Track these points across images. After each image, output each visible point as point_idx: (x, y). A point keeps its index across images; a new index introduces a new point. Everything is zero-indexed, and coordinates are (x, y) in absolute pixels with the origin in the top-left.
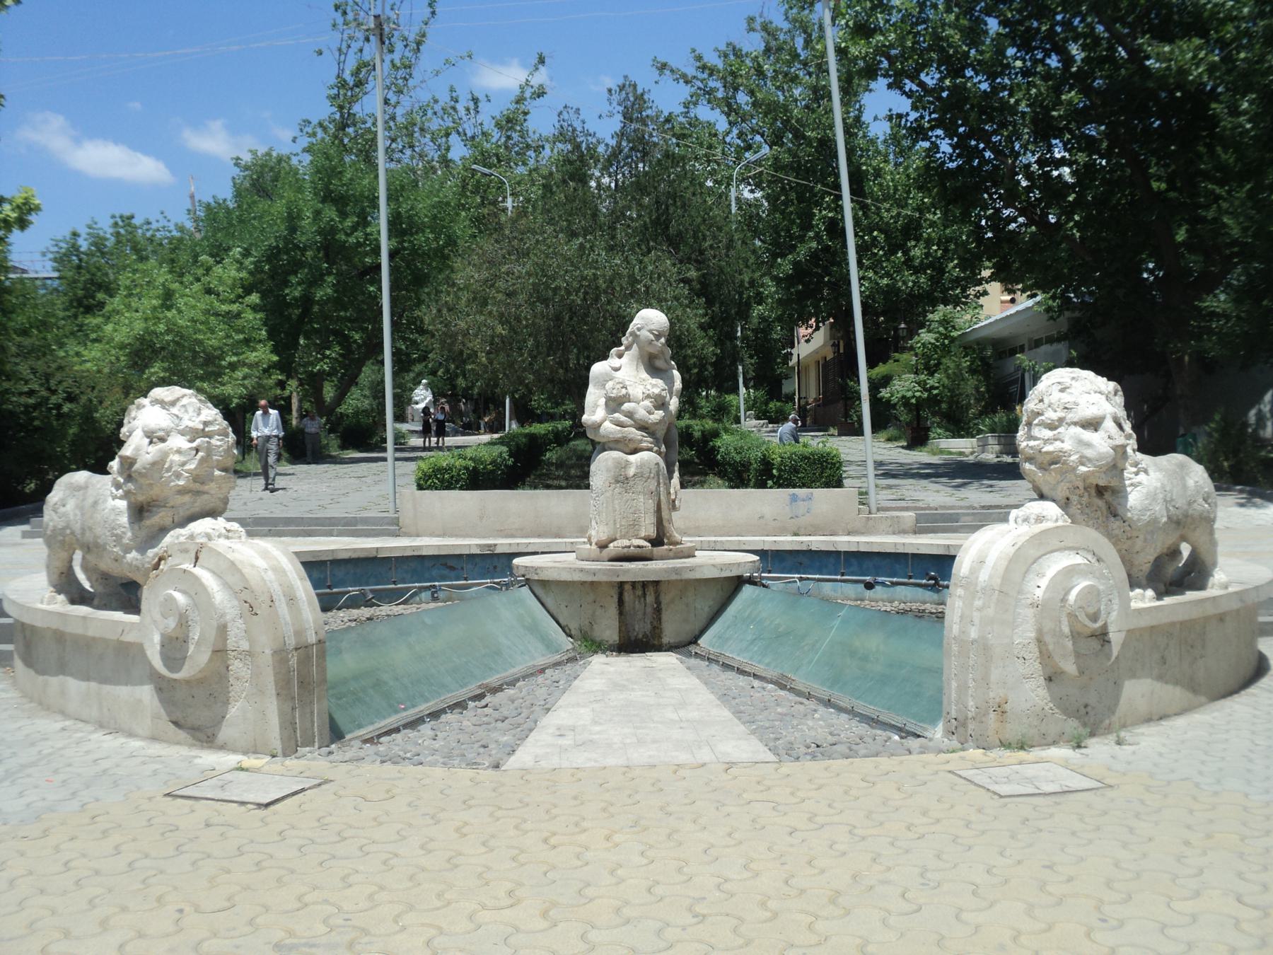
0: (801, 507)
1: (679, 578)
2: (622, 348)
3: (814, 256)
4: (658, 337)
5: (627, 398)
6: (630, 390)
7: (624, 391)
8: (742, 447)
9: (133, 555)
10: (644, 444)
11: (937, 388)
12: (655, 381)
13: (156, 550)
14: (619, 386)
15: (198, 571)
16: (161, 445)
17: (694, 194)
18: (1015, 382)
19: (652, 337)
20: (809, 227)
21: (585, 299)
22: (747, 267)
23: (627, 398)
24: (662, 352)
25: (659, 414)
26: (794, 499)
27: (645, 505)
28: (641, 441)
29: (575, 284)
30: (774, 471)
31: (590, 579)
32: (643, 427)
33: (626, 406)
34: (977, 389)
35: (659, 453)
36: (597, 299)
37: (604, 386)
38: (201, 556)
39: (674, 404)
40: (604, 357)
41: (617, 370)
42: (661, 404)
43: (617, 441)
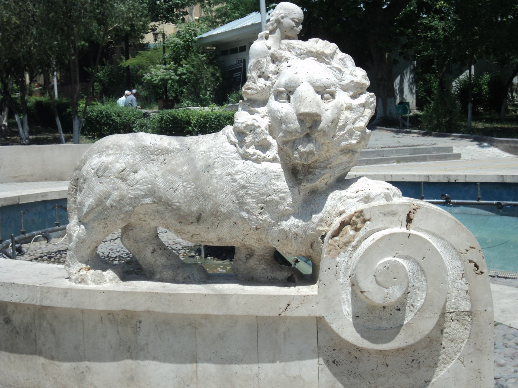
9: (292, 223)
11: (184, 74)
13: (320, 215)
15: (412, 232)
16: (333, 102)
18: (239, 70)
19: (293, 24)
34: (213, 75)
38: (415, 218)
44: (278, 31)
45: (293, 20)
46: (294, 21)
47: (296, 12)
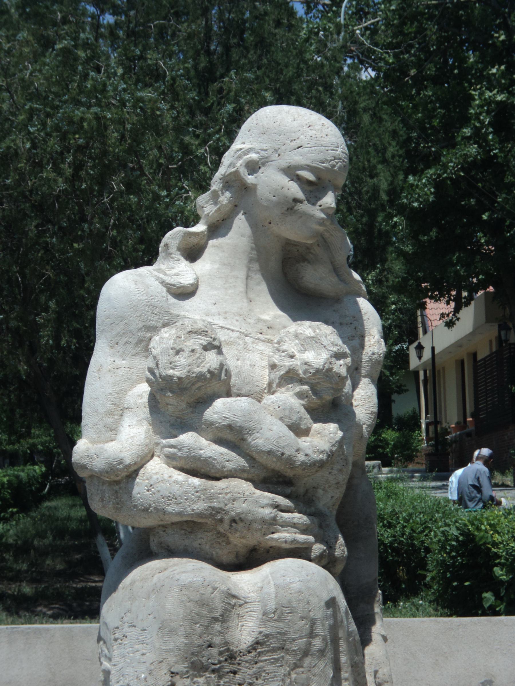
2: (200, 228)
3: (470, 166)
4: (314, 189)
5: (217, 384)
7: (211, 360)
8: (394, 514)
10: (283, 536)
12: (307, 328)
14: (197, 342)
17: (278, 24)
19: (295, 190)
20: (465, 120)
21: (75, 177)
22: (384, 161)
23: (217, 384)
24: (323, 242)
25: (324, 436)
28: (272, 524)
29: (54, 144)
30: (497, 571)
33: (220, 409)
35: (327, 562)
36: (102, 181)
37: (144, 346)
39: (364, 400)
41: (184, 293)
42: (329, 405)
43: (191, 525)
44: (240, 223)
45: (291, 172)
46: (299, 179)
47: (303, 140)
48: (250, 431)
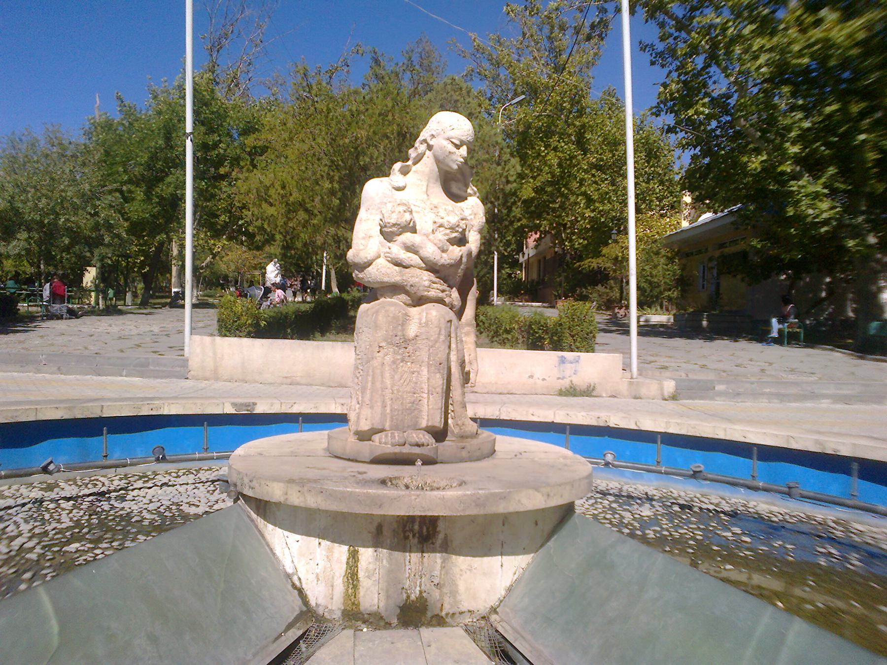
0: (569, 369)
1: (482, 512)
6: (417, 218)
7: (407, 217)
10: (432, 293)
14: (401, 208)
26: (563, 361)
27: (428, 381)
31: (334, 507)
32: (432, 268)
40: (383, 171)
48: (422, 248)
